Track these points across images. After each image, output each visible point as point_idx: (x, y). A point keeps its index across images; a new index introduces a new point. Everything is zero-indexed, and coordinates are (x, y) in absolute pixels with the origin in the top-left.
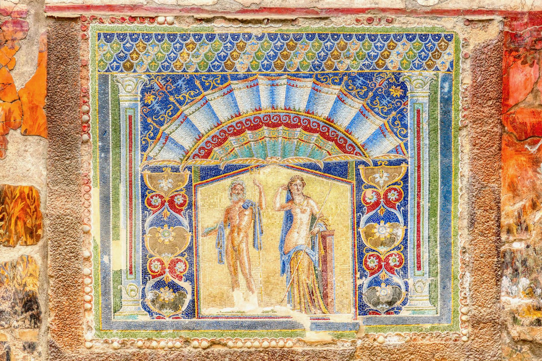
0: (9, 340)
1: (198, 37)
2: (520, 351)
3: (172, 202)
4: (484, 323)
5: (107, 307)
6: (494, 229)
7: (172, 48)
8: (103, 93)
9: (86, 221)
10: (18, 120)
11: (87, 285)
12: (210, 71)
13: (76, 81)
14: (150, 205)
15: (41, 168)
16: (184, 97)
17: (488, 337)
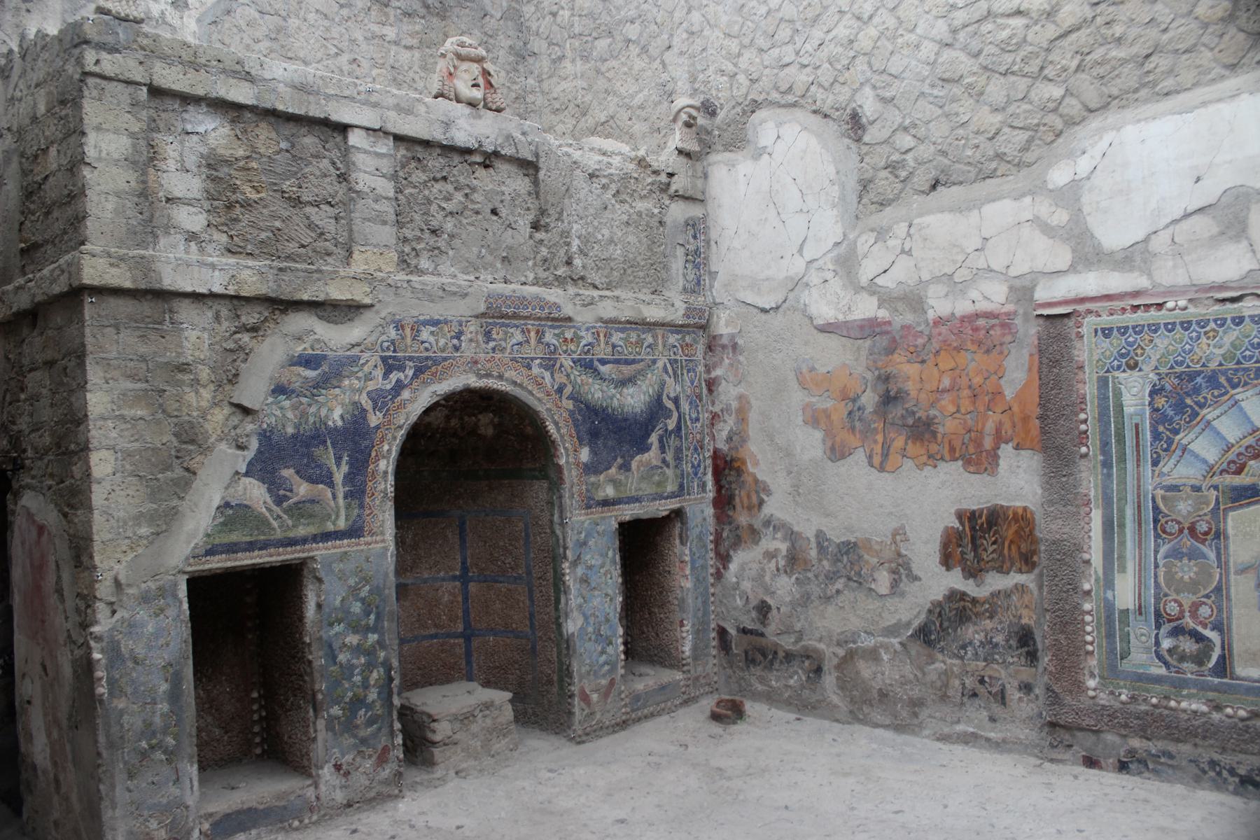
0: (1003, 676)
1: (1221, 322)
3: (1192, 530)
5: (1112, 651)
7: (1186, 339)
8: (1103, 398)
9: (1085, 548)
10: (1010, 432)
11: (1088, 624)
12: (1239, 363)
13: (1072, 386)
14: (1164, 532)
15: (1035, 486)
16: (1205, 398)
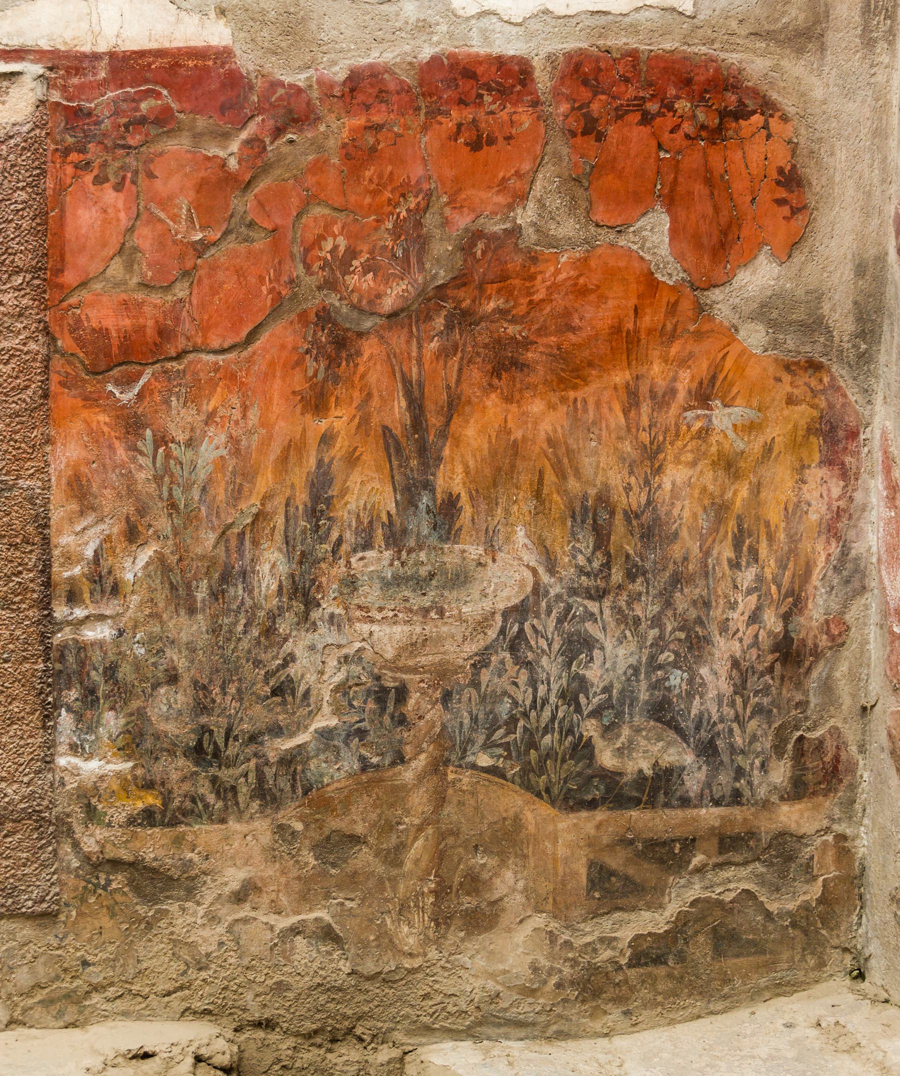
2: (105, 888)
4: (14, 821)
6: (34, 591)
17: (25, 855)
